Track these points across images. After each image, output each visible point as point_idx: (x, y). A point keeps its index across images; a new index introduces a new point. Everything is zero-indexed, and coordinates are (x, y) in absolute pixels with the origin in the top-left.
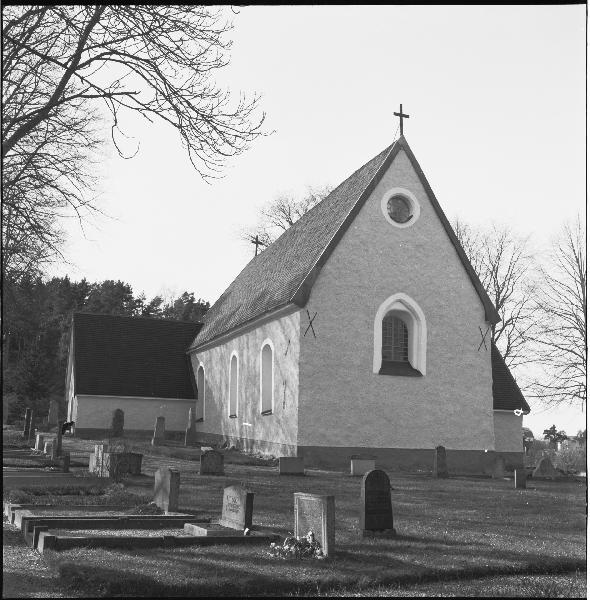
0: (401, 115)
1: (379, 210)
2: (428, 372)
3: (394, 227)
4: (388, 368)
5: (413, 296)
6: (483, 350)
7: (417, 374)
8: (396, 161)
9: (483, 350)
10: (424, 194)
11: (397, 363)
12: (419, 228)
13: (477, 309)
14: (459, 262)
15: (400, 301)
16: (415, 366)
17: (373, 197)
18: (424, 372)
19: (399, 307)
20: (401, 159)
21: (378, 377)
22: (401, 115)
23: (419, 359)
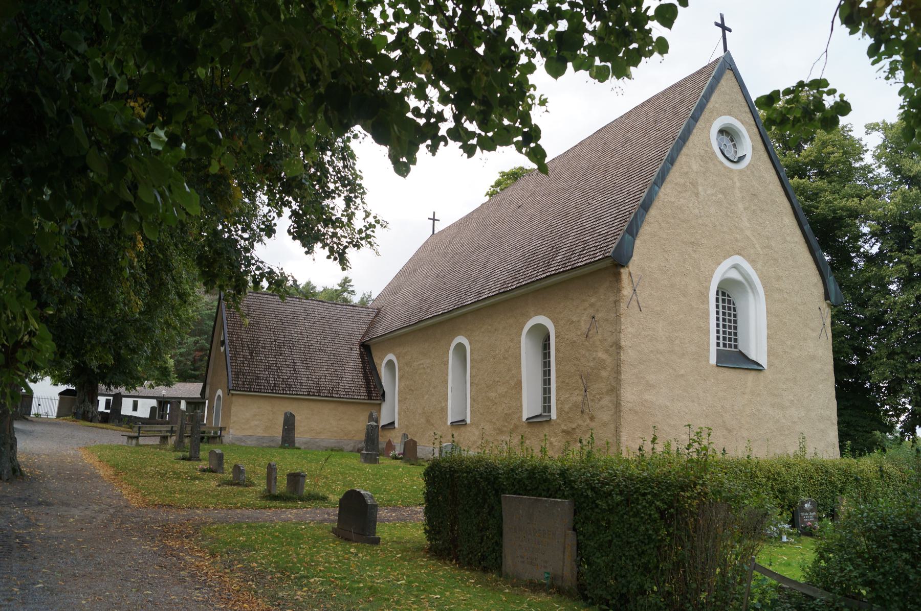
0: (434, 220)
1: (708, 144)
2: (770, 365)
3: (726, 167)
5: (753, 262)
7: (754, 366)
8: (723, 82)
9: (823, 338)
12: (752, 172)
13: (815, 285)
14: (795, 222)
15: (735, 267)
16: (753, 357)
17: (700, 124)
18: (765, 366)
19: (734, 275)
20: (727, 80)
22: (434, 220)
23: (756, 345)
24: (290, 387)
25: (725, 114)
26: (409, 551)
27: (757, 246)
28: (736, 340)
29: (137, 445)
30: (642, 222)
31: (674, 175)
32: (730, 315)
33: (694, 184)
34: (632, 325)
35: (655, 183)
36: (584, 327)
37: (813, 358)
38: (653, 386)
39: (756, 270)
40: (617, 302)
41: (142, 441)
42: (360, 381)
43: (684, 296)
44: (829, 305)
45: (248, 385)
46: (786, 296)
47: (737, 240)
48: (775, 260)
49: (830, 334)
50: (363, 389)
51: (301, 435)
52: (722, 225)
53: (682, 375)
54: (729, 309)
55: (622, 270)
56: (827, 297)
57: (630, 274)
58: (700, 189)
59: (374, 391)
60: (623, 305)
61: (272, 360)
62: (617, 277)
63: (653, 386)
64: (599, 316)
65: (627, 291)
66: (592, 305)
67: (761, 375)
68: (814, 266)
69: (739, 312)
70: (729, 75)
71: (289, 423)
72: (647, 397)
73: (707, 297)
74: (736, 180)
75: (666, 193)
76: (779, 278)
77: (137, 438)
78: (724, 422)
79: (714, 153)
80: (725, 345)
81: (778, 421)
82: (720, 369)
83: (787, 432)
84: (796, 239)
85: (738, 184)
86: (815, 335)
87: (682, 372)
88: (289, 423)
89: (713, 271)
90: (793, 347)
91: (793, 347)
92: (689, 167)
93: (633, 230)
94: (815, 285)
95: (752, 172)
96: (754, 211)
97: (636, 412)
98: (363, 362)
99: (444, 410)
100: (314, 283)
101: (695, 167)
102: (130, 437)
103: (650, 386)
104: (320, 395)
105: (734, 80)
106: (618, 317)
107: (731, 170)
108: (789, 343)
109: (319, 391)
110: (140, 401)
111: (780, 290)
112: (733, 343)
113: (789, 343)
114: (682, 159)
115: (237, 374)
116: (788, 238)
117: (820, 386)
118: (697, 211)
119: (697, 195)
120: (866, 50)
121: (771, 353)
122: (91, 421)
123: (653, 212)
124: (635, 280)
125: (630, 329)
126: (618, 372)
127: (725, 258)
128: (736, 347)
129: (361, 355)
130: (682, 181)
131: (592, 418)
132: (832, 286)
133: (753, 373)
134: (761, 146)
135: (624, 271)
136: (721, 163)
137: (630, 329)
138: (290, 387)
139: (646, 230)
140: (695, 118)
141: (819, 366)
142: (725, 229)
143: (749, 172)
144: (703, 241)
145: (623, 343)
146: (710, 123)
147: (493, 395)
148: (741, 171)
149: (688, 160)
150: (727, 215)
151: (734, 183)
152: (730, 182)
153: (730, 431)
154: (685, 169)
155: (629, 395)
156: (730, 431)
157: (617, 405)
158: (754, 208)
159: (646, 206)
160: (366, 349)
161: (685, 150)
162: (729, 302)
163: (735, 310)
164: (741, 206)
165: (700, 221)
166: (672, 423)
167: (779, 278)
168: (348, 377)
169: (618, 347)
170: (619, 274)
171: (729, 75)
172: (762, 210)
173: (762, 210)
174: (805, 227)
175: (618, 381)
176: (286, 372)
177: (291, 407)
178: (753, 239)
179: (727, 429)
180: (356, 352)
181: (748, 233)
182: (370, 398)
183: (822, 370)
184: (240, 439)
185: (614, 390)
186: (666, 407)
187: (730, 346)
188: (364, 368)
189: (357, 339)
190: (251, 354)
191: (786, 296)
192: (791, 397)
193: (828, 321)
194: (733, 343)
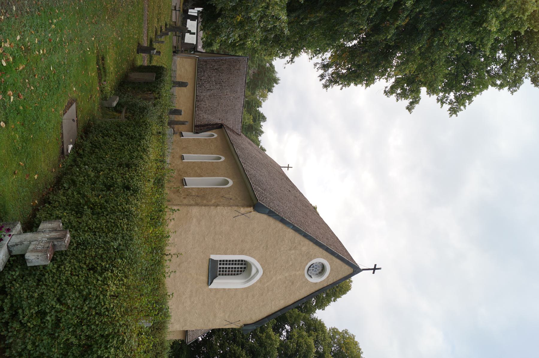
0: (288, 167)
1: (315, 257)
2: (211, 290)
3: (305, 266)
4: (213, 264)
5: (260, 280)
6: (225, 323)
7: (210, 282)
8: (347, 267)
9: (225, 323)
11: (215, 270)
12: (304, 282)
13: (251, 319)
15: (257, 271)
16: (215, 281)
17: (325, 253)
18: (210, 287)
19: (254, 271)
21: (208, 259)
22: (288, 167)
23: (221, 283)
24: (200, 87)
25: (331, 267)
26: (134, 60)
27: (268, 283)
28: (223, 275)
29: (172, 10)
30: (275, 218)
31: (299, 238)
32: (235, 271)
33: (295, 248)
34: (227, 213)
35: (294, 226)
36: (227, 196)
37: (215, 316)
38: (199, 224)
39: (257, 282)
40: (237, 206)
41: (174, 12)
42: (204, 122)
43: (242, 241)
44: (241, 326)
45: (201, 67)
46: (245, 300)
47: (270, 272)
48: (262, 295)
49: (227, 327)
50: (199, 123)
51: (177, 90)
52: (277, 263)
53: (204, 239)
54: (238, 271)
55: (252, 208)
56: (245, 325)
57: (251, 212)
58: (293, 251)
59: (199, 128)
60: (236, 208)
61: (213, 79)
62: (250, 206)
63: (199, 224)
64: (231, 201)
65: (243, 210)
66: (237, 199)
67: (206, 284)
68: (260, 318)
69: (236, 276)
70: (351, 270)
71: (183, 84)
72: (194, 220)
73: (242, 254)
74: (299, 272)
75: (290, 233)
76: (253, 296)
77: (175, 10)
78: (183, 262)
79: (311, 260)
80: (220, 268)
81: (184, 294)
84: (273, 308)
85: (297, 273)
87: (206, 239)
88: (183, 84)
89: (254, 258)
90: (220, 304)
91: (220, 304)
92: (303, 246)
93: (271, 214)
94: (251, 319)
95: (304, 282)
96: (285, 282)
97: (187, 214)
98: (213, 125)
99: (189, 153)
100: (263, 135)
101: (304, 249)
102: (175, 7)
104: (197, 101)
105: (349, 273)
106: (231, 206)
107: (304, 270)
108: (222, 301)
109: (198, 101)
110: (195, 36)
111: (247, 296)
112: (221, 273)
113: (222, 301)
114: (307, 242)
115: (206, 62)
116: (273, 303)
117: (201, 320)
118: (282, 249)
119: (290, 250)
120: (349, 293)
121: (217, 290)
122: (183, 4)
123: (280, 225)
125: (225, 212)
126: (205, 206)
127: (261, 265)
128: (220, 274)
129: (217, 124)
130: (296, 242)
131: (184, 198)
132: (251, 328)
133: (207, 280)
135: (251, 209)
136: (307, 264)
137: (225, 212)
138: (200, 87)
139: (271, 221)
140: (327, 250)
141: (211, 319)
143: (304, 280)
145: (218, 207)
147: (196, 168)
148: (304, 275)
149: (307, 246)
150: (282, 267)
151: (298, 271)
153: (179, 265)
154: (302, 244)
155: (195, 211)
156: (179, 265)
157: (191, 205)
158: (287, 282)
159: (282, 221)
160: (220, 127)
161: (311, 243)
162: (241, 271)
163: (238, 274)
164: (287, 275)
166: (182, 234)
167: (253, 296)
168: (206, 116)
169: (217, 205)
170: (250, 206)
171: (351, 270)
172: (286, 287)
173: (286, 287)
174: (279, 312)
175: (202, 205)
176: (208, 86)
177: (190, 87)
179: (180, 264)
180: (218, 121)
181: (274, 278)
182: (196, 126)
183: (209, 321)
184: (175, 63)
185: (197, 204)
186: (190, 231)
187: (220, 271)
188: (210, 125)
189: (225, 122)
190: (216, 69)
191: (245, 300)
193: (234, 326)
194: (221, 273)
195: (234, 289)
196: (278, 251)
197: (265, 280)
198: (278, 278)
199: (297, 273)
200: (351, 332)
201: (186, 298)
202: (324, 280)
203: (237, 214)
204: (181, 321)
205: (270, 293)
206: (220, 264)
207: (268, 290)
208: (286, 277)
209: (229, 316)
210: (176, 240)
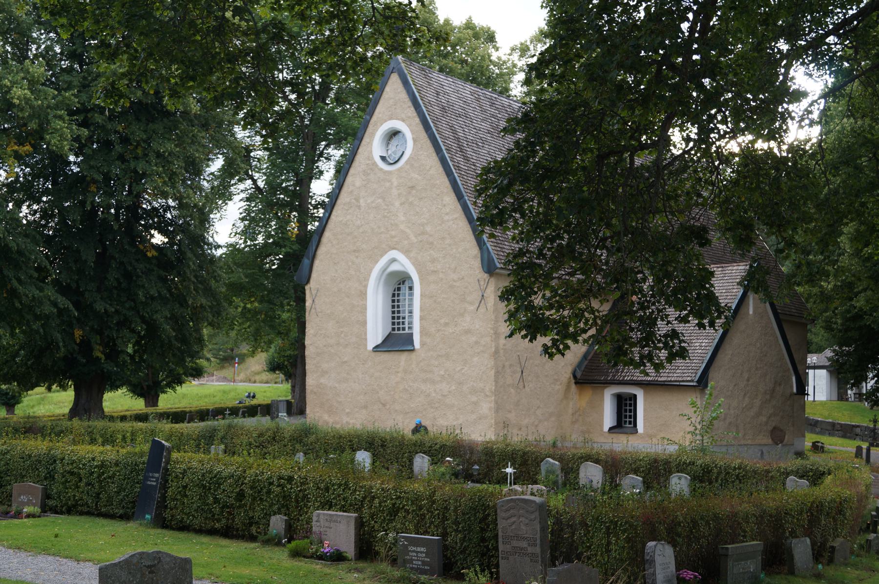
1: (370, 157)
6: (482, 310)
10: (417, 120)
15: (394, 260)
21: (374, 354)
37: (468, 332)
38: (327, 372)
46: (441, 275)
48: (432, 243)
53: (346, 362)
58: (362, 201)
63: (327, 372)
72: (322, 380)
79: (375, 164)
82: (379, 353)
83: (437, 405)
84: (455, 216)
85: (395, 184)
86: (472, 308)
87: (346, 359)
90: (446, 324)
91: (446, 324)
96: (411, 203)
101: (358, 184)
103: (324, 373)
107: (390, 173)
108: (442, 321)
117: (476, 359)
118: (359, 222)
119: (359, 207)
124: (314, 292)
127: (382, 256)
133: (406, 353)
134: (423, 135)
136: (381, 169)
141: (474, 339)
142: (382, 230)
144: (364, 246)
146: (373, 135)
150: (385, 217)
152: (388, 184)
153: (384, 405)
164: (397, 204)
165: (361, 230)
166: (340, 400)
167: (433, 260)
178: (408, 230)
181: (402, 227)
183: (477, 343)
186: (335, 388)
191: (441, 275)
192: (442, 373)
195: (421, 299)
196: (361, 230)
197: (406, 242)
198: (403, 218)
199: (395, 184)
200: (492, 29)
201: (435, 391)
202: (409, 126)
203: (313, 311)
204: (474, 399)
205: (428, 229)
206: (404, 329)
207: (423, 233)
208: (401, 204)
209: (471, 303)
210: (347, 410)
